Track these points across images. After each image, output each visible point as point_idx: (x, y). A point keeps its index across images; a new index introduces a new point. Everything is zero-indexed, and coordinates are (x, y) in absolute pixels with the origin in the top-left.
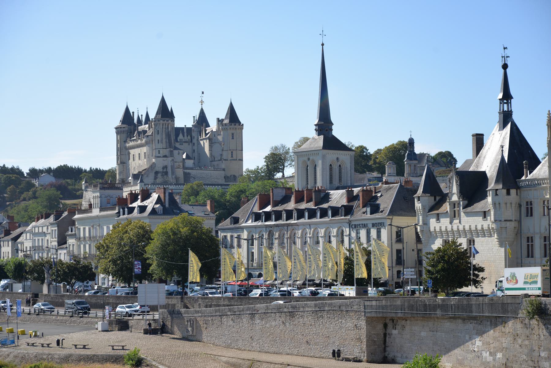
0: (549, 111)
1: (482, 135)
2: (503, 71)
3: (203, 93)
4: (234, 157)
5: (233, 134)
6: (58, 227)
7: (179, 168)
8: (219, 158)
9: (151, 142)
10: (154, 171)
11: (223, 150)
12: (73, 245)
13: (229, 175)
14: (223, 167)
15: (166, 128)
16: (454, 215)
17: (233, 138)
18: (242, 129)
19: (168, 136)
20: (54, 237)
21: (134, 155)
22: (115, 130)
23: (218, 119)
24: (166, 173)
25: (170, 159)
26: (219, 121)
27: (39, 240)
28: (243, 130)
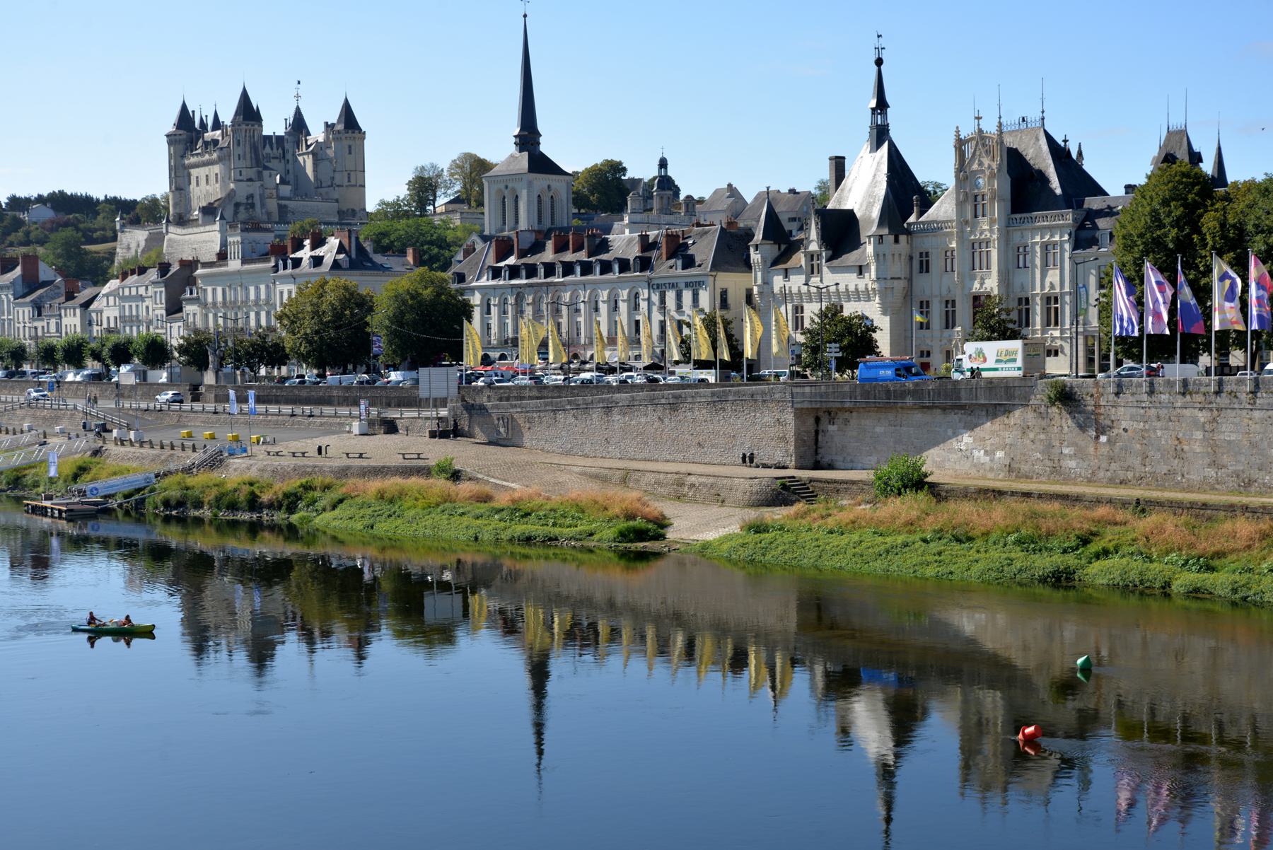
0: (958, 127)
1: (843, 158)
2: (876, 68)
3: (299, 82)
4: (353, 182)
5: (350, 147)
6: (166, 287)
7: (271, 198)
8: (330, 183)
9: (227, 158)
10: (233, 202)
11: (334, 171)
12: (194, 314)
13: (345, 209)
14: (336, 196)
15: (250, 136)
16: (812, 270)
17: (350, 153)
18: (364, 138)
19: (254, 148)
20: (158, 301)
21: (197, 177)
22: (165, 138)
23: (327, 123)
24: (252, 206)
25: (258, 184)
26: (329, 127)
27: (131, 306)
28: (365, 141)
